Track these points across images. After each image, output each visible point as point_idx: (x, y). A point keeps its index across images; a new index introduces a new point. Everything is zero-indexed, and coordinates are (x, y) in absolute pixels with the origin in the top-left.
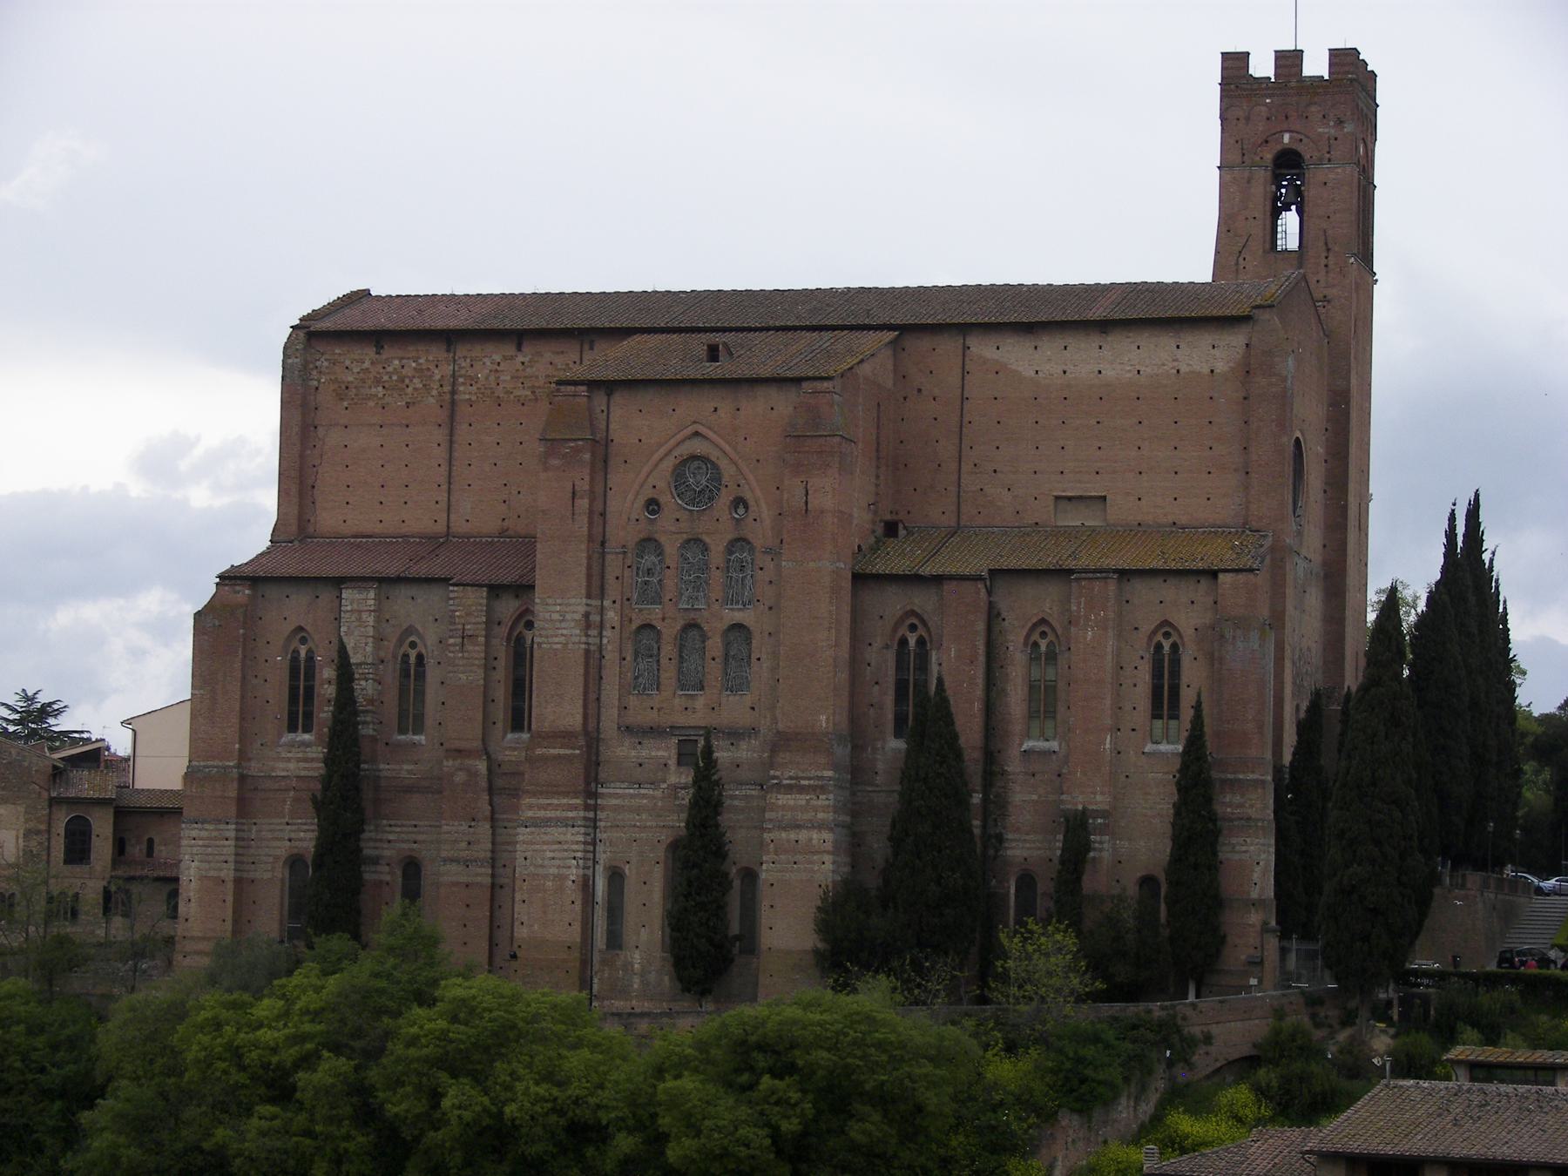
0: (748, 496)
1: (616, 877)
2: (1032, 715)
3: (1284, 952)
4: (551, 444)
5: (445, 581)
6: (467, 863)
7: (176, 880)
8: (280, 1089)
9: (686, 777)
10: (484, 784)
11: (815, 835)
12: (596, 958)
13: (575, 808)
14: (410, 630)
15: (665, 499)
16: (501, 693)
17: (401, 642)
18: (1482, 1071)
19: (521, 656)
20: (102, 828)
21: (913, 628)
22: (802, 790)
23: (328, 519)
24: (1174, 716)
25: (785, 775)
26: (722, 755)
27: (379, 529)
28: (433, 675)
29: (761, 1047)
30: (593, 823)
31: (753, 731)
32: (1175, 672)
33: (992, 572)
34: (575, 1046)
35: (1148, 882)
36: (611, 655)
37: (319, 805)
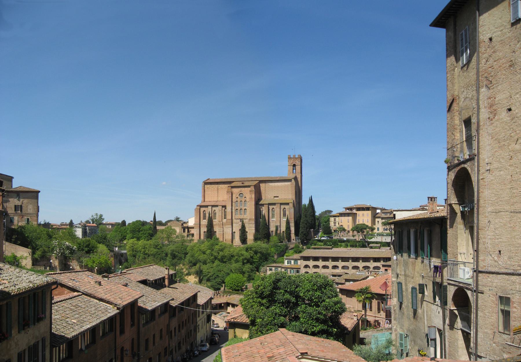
2: (272, 217)
3: (296, 238)
9: (241, 223)
14: (215, 210)
16: (223, 216)
19: (225, 212)
24: (285, 216)
26: (244, 221)
28: (217, 214)
29: (249, 248)
31: (247, 219)
32: (285, 212)
33: (269, 203)
35: (283, 232)
37: (207, 227)
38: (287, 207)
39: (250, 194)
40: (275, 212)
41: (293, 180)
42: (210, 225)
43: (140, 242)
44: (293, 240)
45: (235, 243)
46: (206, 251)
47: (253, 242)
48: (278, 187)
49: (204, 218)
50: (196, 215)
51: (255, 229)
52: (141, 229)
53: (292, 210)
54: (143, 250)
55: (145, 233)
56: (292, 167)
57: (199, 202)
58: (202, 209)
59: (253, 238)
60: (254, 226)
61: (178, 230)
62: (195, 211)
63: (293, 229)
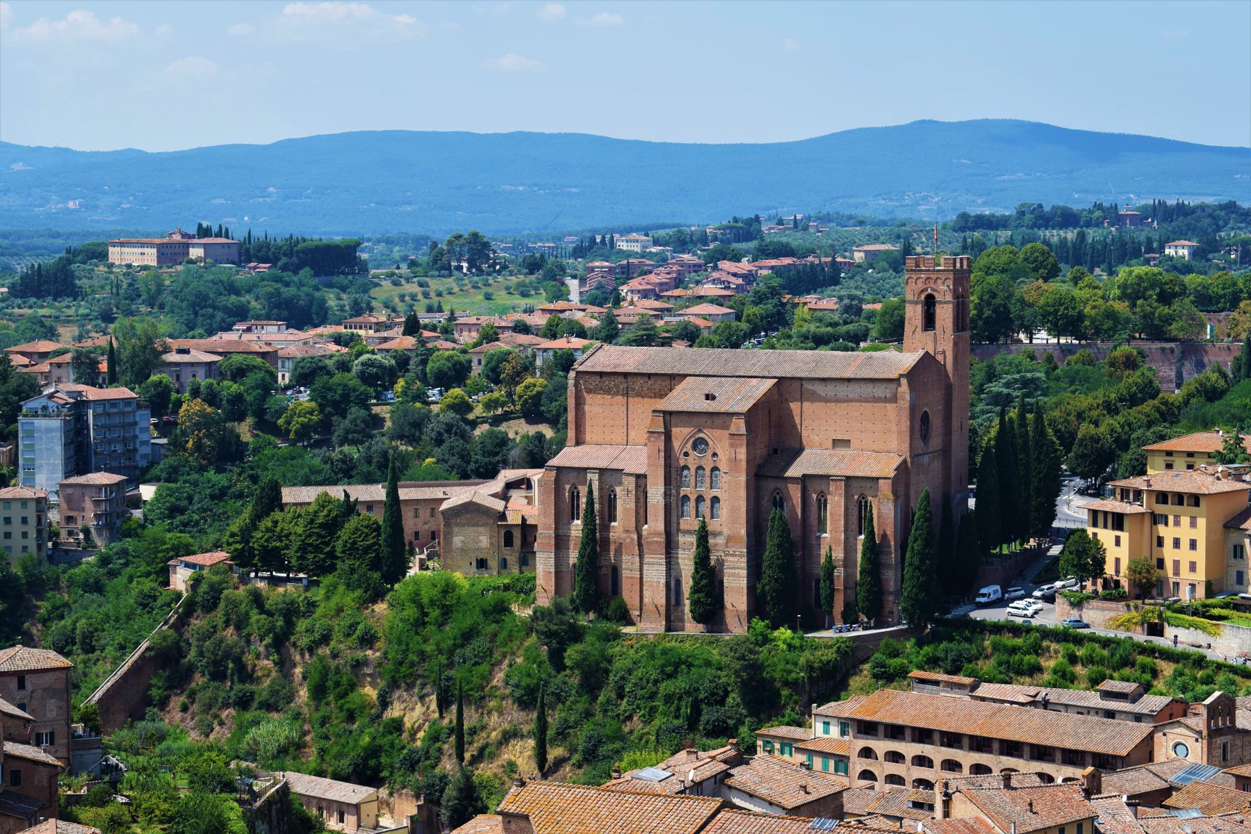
0: (718, 452)
10: (636, 542)
15: (690, 452)
26: (711, 541)
31: (720, 533)
33: (804, 476)
36: (674, 505)
39: (732, 445)
60: (745, 565)
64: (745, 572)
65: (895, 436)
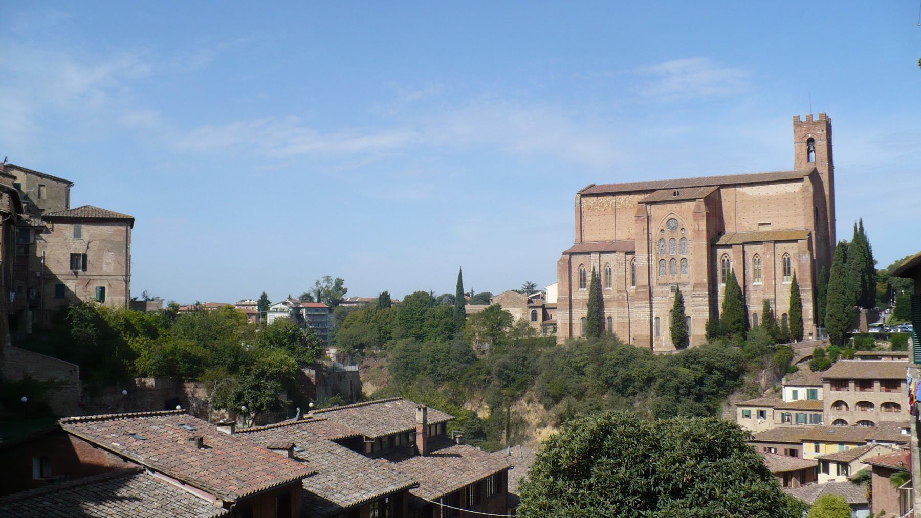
0: (684, 227)
1: (657, 318)
3: (818, 331)
4: (638, 217)
5: (614, 252)
6: (623, 317)
7: (556, 324)
8: (580, 371)
9: (673, 295)
11: (704, 307)
12: (654, 338)
13: (647, 303)
16: (629, 277)
17: (605, 266)
18: (863, 357)
20: (540, 312)
21: (726, 257)
22: (700, 297)
23: (587, 238)
25: (697, 293)
27: (599, 240)
28: (613, 273)
30: (651, 307)
31: (688, 283)
32: (789, 264)
34: (649, 359)
35: (785, 315)
36: (654, 266)
37: (588, 306)
38: (792, 248)
39: (696, 220)
40: (762, 263)
41: (807, 179)
42: (597, 303)
43: (424, 346)
44: (811, 334)
45: (659, 346)
46: (584, 366)
47: (705, 342)
48: (768, 199)
49: (582, 284)
50: (561, 277)
51: (710, 311)
52: (425, 316)
53: (807, 259)
54: (430, 366)
55: (436, 323)
56: (805, 147)
57: (569, 243)
58: (577, 260)
59: (704, 332)
61: (518, 314)
62: (559, 265)
63: (808, 308)
64: (708, 308)
65: (802, 217)
